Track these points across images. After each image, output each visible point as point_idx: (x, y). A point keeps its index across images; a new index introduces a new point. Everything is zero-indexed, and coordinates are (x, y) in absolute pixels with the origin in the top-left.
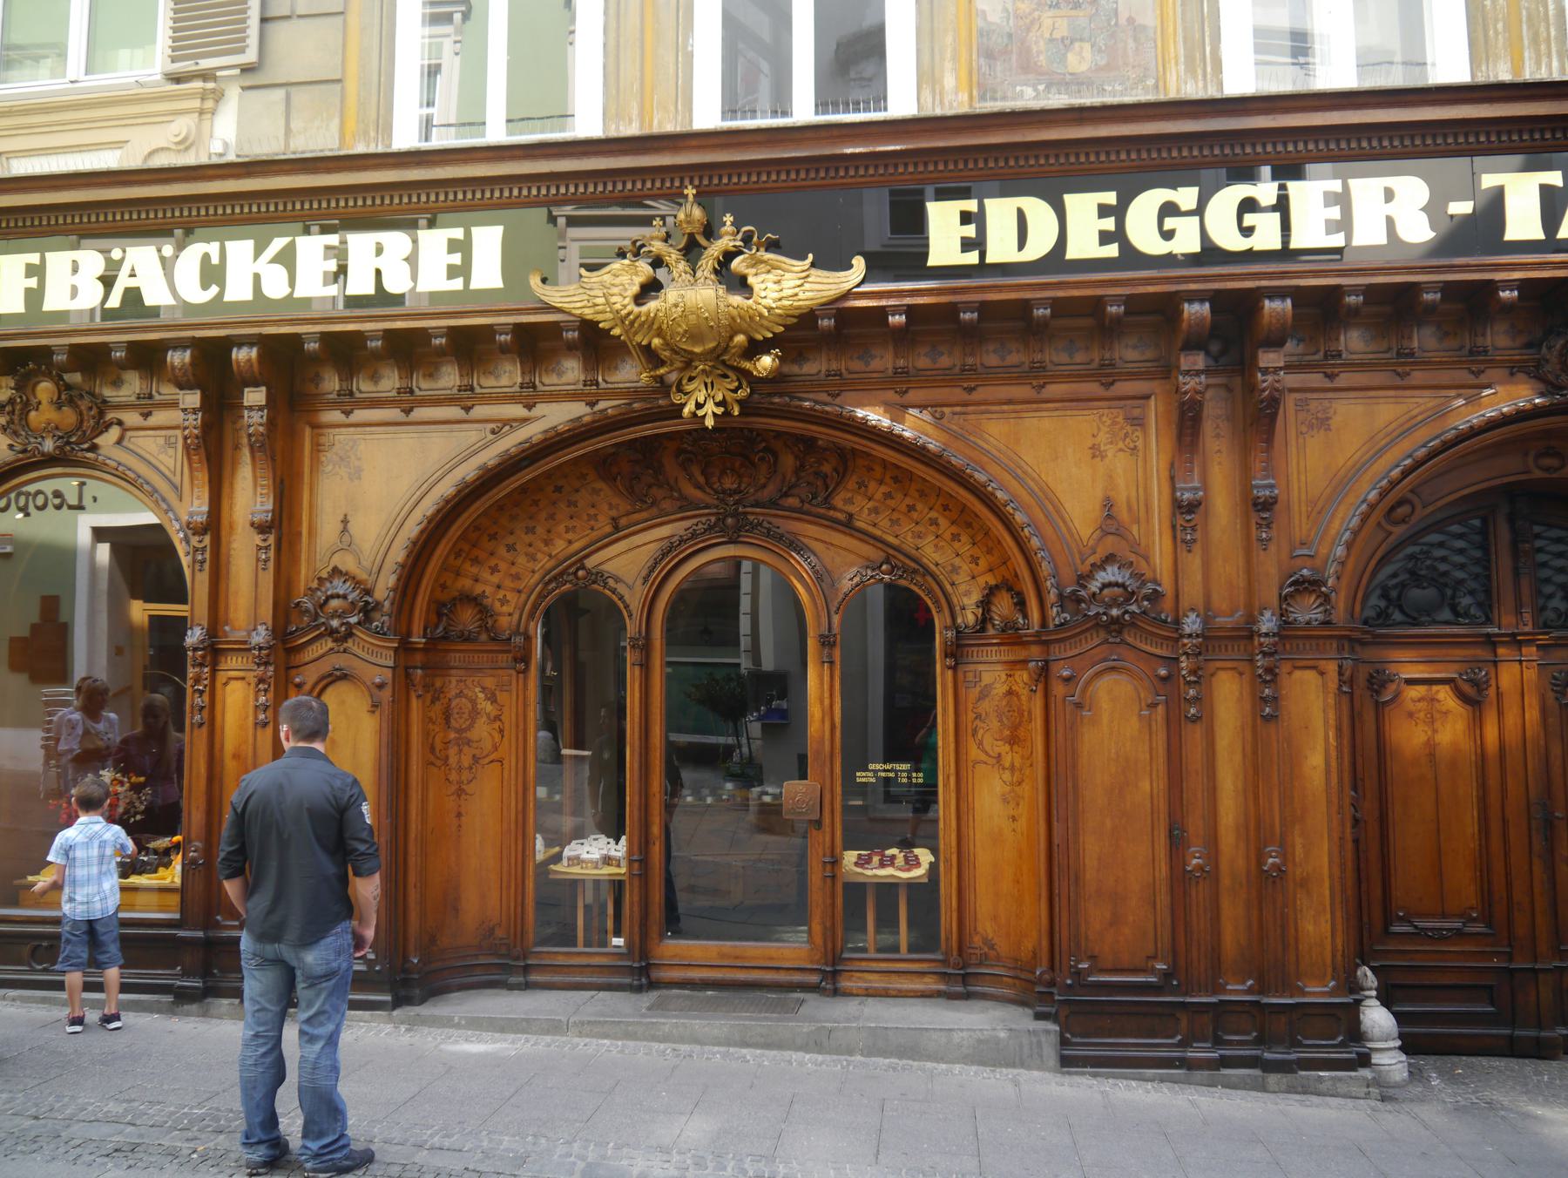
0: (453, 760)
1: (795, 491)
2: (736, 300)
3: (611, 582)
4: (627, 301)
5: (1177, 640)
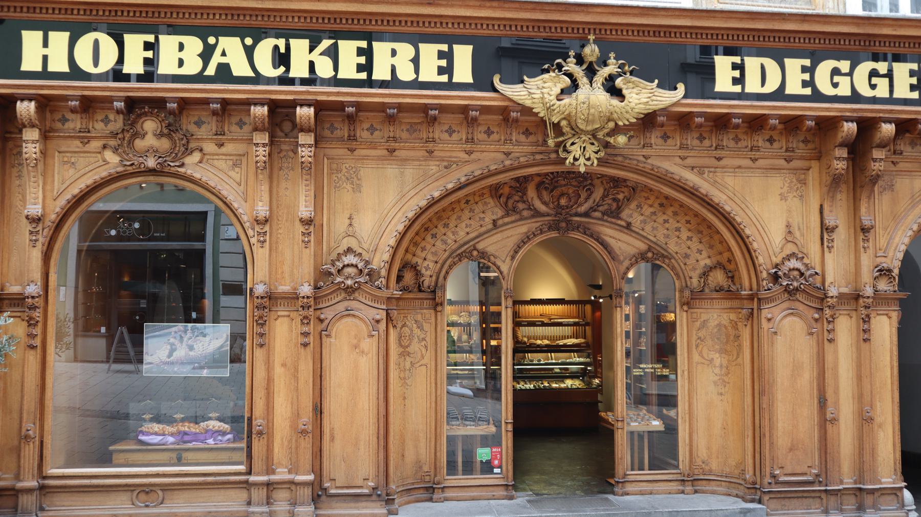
0: (402, 365)
1: (601, 208)
2: (615, 102)
3: (492, 258)
4: (552, 98)
5: (822, 299)
